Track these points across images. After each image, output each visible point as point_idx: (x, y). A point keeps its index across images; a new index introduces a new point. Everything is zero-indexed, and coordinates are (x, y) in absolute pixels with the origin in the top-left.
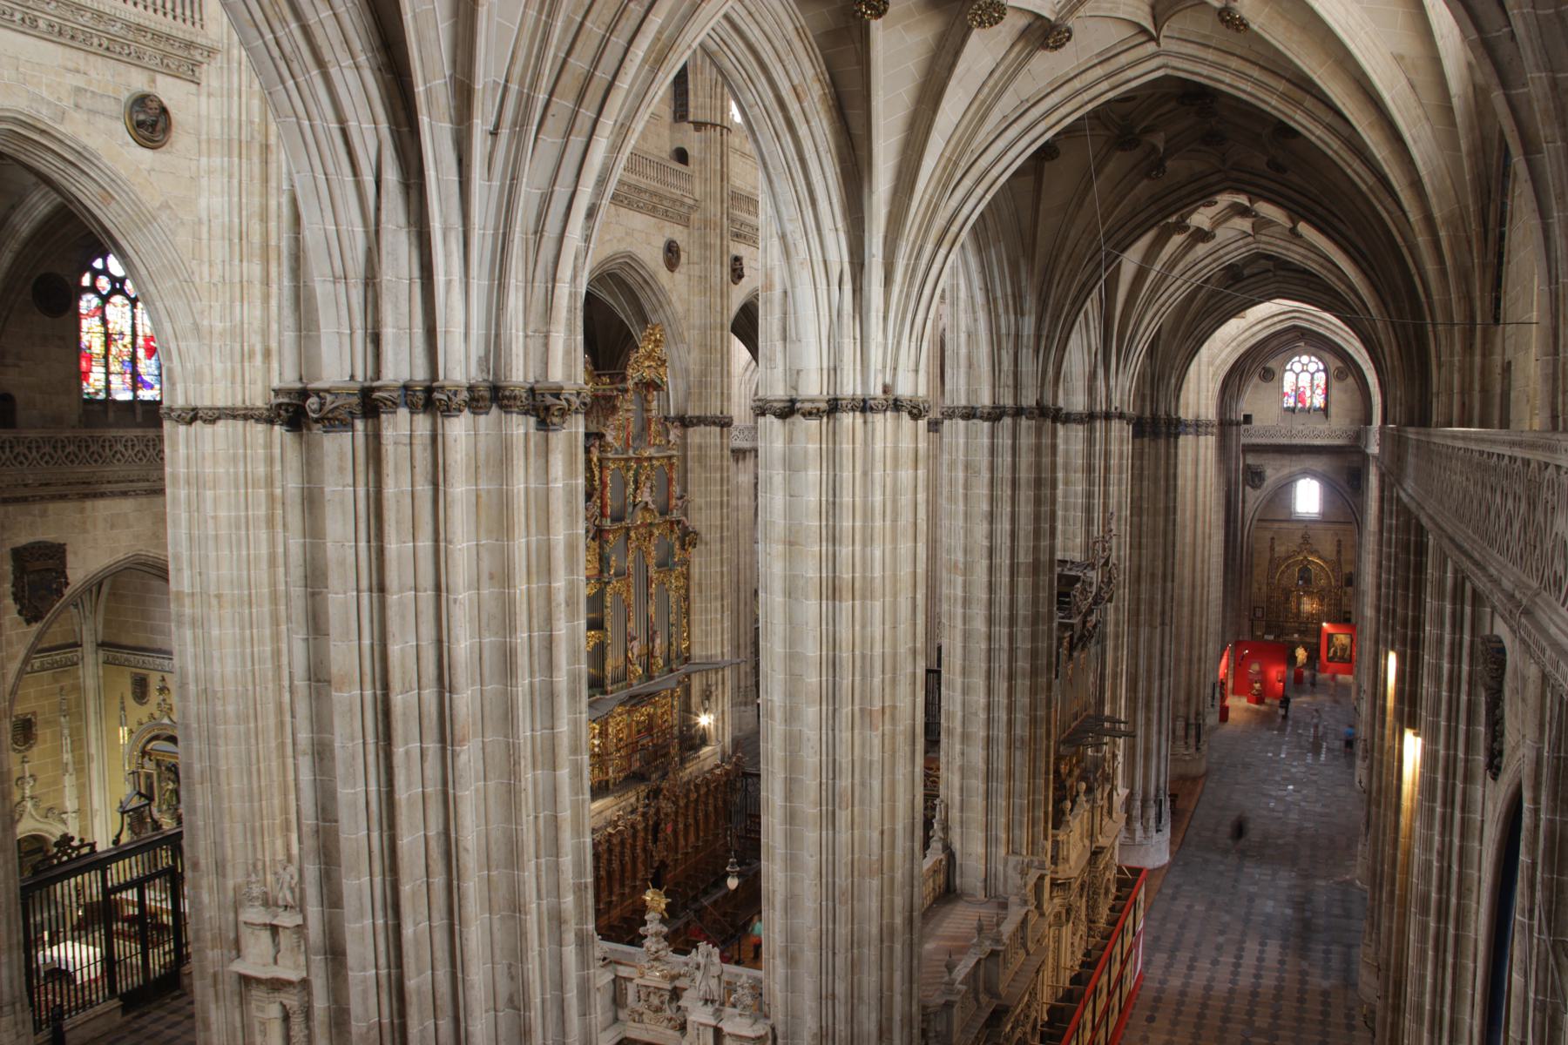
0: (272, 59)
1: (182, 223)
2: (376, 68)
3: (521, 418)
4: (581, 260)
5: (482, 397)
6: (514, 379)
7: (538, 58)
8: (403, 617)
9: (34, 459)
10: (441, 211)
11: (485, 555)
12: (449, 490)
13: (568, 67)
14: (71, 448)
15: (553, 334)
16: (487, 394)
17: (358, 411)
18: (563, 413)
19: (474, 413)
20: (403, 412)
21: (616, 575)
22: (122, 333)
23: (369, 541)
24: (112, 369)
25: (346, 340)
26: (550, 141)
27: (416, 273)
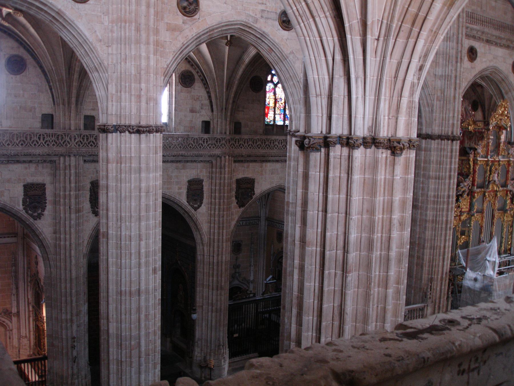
0: (296, 16)
1: (298, 59)
2: (333, 17)
3: (384, 150)
4: (416, 87)
5: (369, 142)
6: (381, 136)
7: (393, 10)
8: (332, 223)
9: (246, 146)
10: (355, 71)
11: (365, 203)
12: (353, 177)
13: (409, 11)
14: (259, 143)
15: (399, 118)
16: (370, 141)
17: (322, 145)
18: (402, 150)
19: (366, 148)
20: (338, 147)
21: (477, 212)
22: (281, 99)
23: (323, 193)
24: (277, 112)
25: (320, 118)
26: (401, 41)
27: (346, 94)
